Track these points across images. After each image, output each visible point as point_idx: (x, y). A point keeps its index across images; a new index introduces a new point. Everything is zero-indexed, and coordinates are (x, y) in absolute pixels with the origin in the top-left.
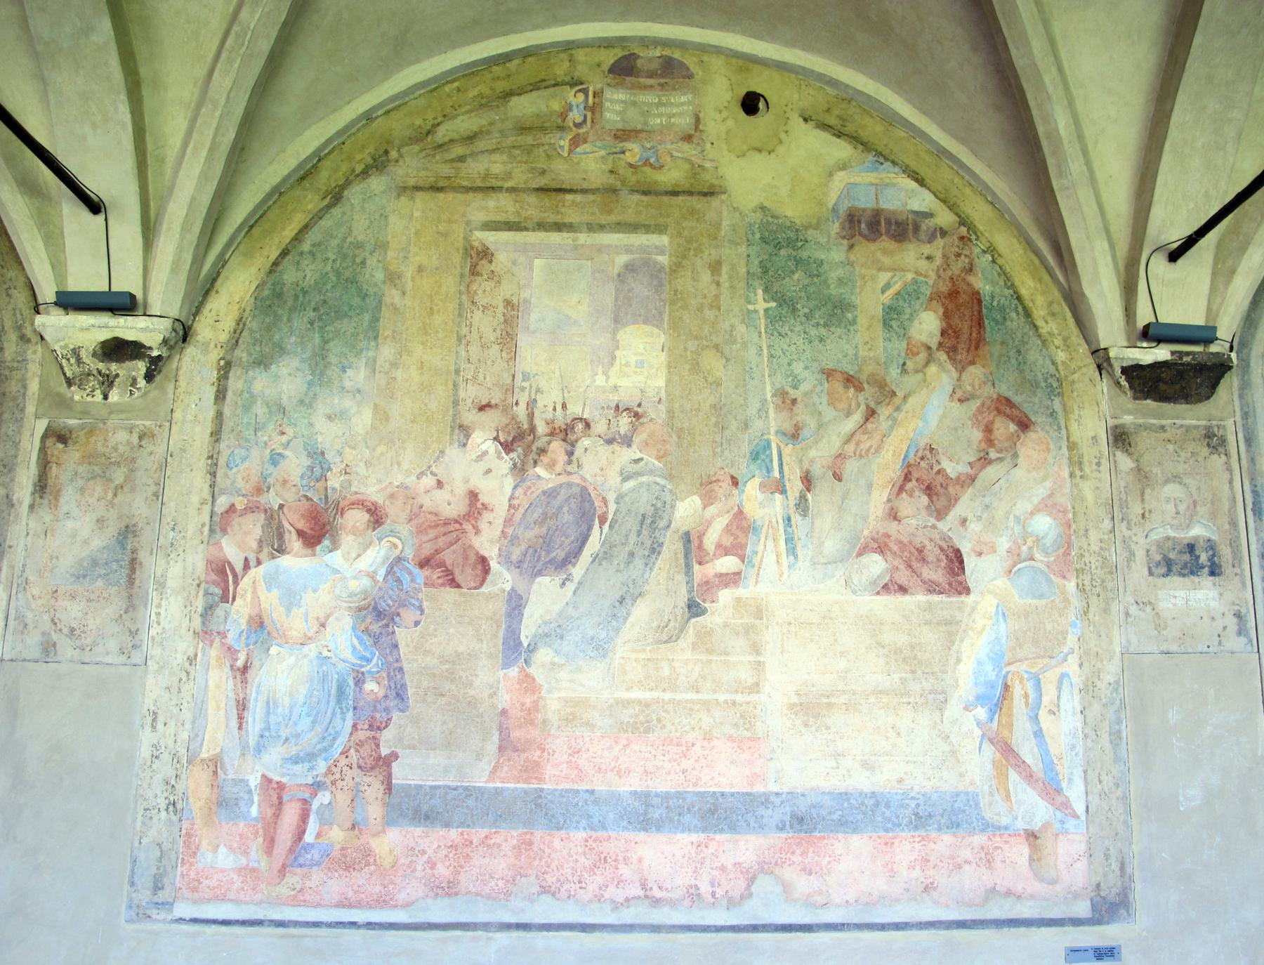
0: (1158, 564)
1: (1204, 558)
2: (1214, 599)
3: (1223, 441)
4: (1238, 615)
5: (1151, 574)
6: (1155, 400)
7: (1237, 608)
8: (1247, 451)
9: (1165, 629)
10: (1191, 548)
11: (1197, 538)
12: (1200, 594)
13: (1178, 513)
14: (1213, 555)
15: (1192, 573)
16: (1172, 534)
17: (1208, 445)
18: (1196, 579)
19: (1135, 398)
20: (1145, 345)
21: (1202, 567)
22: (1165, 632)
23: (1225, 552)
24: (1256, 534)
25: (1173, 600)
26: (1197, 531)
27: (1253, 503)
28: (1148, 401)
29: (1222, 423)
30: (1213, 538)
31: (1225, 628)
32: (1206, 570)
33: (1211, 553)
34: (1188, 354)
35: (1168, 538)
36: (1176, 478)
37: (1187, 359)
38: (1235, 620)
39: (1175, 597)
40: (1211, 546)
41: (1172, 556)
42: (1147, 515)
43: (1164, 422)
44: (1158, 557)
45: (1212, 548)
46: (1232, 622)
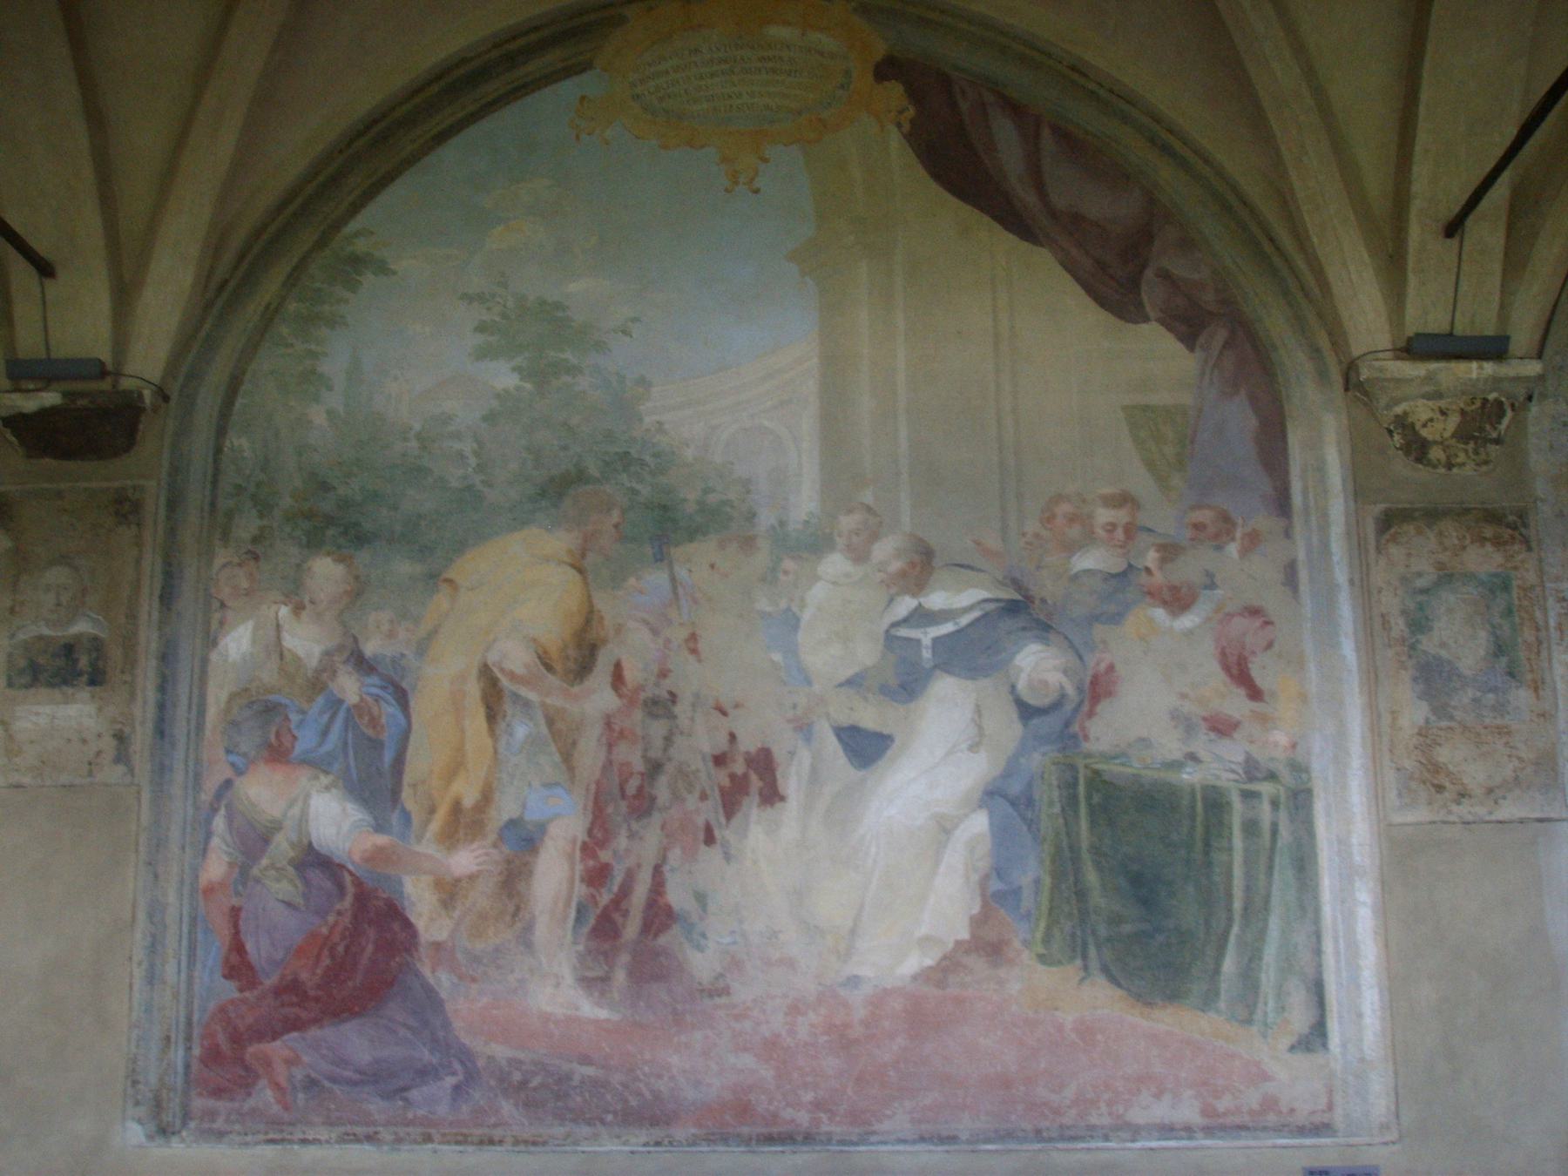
0: (21, 672)
1: (84, 662)
2: (90, 716)
3: (137, 507)
4: (120, 738)
5: (10, 685)
6: (56, 458)
7: (119, 726)
8: (168, 518)
9: (16, 756)
10: (69, 649)
11: (79, 637)
12: (72, 710)
13: (58, 605)
14: (97, 659)
15: (65, 682)
16: (47, 632)
17: (117, 513)
18: (70, 691)
19: (30, 457)
20: (31, 386)
21: (80, 674)
22: (17, 760)
23: (115, 654)
24: (160, 629)
25: (34, 718)
26: (82, 627)
27: (163, 588)
28: (47, 460)
29: (142, 482)
30: (102, 635)
31: (99, 753)
32: (85, 678)
33: (94, 655)
34: (82, 395)
35: (40, 638)
36: (64, 559)
37: (82, 402)
38: (114, 743)
39: (37, 714)
40: (96, 645)
41: (41, 660)
42: (17, 609)
43: (62, 486)
44: (22, 663)
45: (97, 650)
46: (108, 744)
